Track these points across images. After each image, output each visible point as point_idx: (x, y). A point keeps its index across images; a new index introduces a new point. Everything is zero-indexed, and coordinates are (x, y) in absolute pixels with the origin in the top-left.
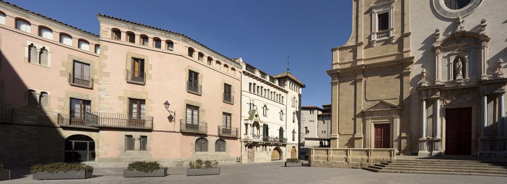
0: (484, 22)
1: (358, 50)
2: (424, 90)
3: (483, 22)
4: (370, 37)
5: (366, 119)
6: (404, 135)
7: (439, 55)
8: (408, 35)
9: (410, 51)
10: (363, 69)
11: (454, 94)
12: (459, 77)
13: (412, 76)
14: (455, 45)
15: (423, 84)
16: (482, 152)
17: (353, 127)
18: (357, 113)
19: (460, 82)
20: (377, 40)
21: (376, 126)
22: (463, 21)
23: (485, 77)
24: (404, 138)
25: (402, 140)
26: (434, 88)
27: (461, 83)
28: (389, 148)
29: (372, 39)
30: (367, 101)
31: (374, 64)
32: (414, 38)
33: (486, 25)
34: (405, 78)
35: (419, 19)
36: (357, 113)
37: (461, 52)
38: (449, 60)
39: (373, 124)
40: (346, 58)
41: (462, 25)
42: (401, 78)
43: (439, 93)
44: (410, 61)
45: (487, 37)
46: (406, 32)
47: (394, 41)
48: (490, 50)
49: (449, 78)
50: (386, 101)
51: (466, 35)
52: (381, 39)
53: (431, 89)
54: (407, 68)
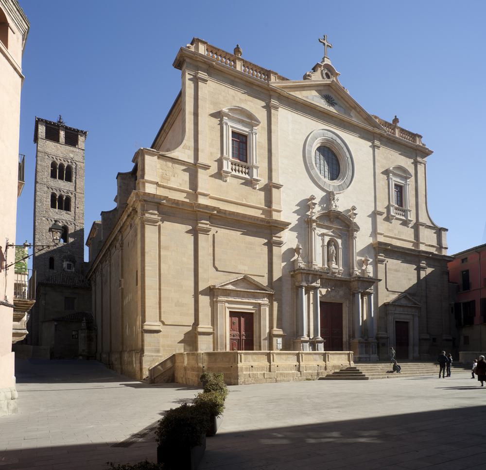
4: (220, 162)
5: (217, 302)
6: (277, 331)
10: (212, 214)
13: (284, 248)
16: (361, 356)
17: (192, 311)
18: (200, 289)
21: (232, 314)
23: (357, 272)
24: (278, 336)
25: (275, 339)
26: (312, 274)
28: (253, 350)
30: (217, 270)
31: (233, 213)
34: (275, 249)
35: (290, 170)
36: (200, 289)
38: (323, 240)
39: (228, 311)
40: (173, 179)
42: (270, 245)
43: (319, 281)
44: (282, 226)
47: (258, 187)
50: (249, 276)
51: (340, 217)
53: (312, 274)
54: (277, 235)
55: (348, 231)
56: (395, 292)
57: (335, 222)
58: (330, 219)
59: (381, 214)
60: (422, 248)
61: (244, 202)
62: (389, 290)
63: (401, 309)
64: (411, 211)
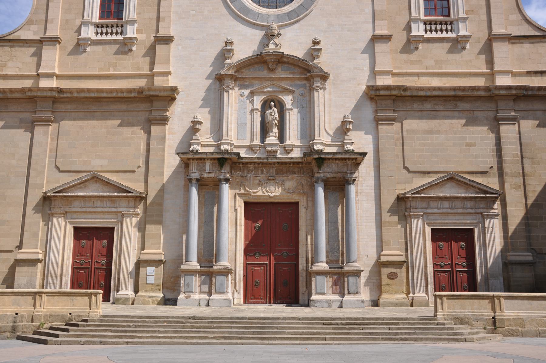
0: (319, 43)
1: (44, 51)
2: (194, 159)
3: (316, 42)
7: (230, 91)
8: (167, 40)
9: (169, 73)
11: (262, 173)
12: (272, 139)
14: (265, 73)
15: (195, 146)
19: (274, 148)
20: (94, 37)
22: (279, 34)
27: (275, 152)
29: (83, 35)
32: (180, 48)
33: (319, 50)
37: (275, 90)
40: (10, 64)
41: (277, 40)
45: (322, 70)
46: (161, 33)
48: (330, 94)
49: (252, 140)
50: (103, 174)
52: (104, 37)
55: (307, 79)
56: (429, 172)
57: (280, 69)
58: (269, 69)
59: (387, 38)
60: (502, 81)
61: (112, 72)
62: (410, 170)
63: (446, 204)
64: (467, 19)
